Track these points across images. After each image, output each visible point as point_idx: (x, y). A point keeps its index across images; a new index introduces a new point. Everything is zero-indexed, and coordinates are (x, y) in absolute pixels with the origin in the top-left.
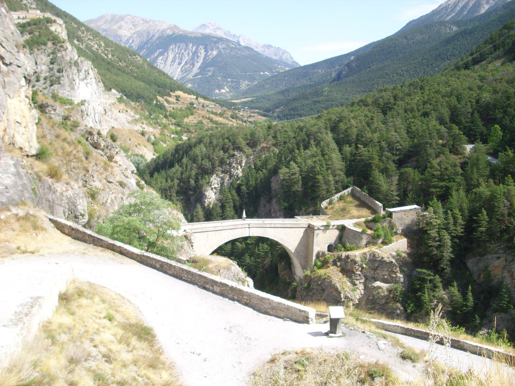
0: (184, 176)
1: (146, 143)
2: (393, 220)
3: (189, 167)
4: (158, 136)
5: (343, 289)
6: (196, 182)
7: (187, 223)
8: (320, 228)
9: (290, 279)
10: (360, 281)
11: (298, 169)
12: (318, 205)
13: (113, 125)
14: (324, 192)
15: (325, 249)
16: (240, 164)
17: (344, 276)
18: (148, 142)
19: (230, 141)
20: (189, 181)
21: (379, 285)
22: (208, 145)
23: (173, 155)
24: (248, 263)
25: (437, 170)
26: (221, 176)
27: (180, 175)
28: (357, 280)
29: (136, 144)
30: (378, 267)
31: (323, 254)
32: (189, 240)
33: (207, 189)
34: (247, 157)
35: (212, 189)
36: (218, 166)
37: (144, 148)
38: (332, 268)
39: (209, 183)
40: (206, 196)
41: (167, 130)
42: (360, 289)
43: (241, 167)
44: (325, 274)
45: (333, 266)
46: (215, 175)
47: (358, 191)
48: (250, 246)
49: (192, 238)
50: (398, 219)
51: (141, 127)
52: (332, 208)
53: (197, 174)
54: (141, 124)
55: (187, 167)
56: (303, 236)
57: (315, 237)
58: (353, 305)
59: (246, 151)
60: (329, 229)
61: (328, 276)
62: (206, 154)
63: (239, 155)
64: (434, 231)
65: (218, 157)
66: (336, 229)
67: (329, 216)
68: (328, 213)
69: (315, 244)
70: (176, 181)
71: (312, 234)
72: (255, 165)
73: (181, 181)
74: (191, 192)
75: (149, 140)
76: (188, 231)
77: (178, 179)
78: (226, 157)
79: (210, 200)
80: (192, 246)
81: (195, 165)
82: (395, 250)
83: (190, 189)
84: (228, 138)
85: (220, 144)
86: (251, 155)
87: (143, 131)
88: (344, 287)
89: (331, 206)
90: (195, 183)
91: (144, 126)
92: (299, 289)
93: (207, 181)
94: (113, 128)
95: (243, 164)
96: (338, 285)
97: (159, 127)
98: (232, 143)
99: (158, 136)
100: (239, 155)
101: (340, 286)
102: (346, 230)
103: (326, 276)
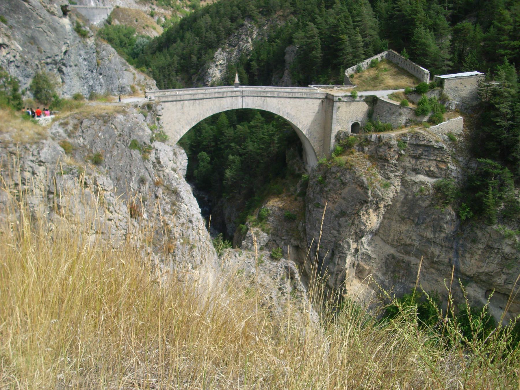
0: (185, 52)
1: (155, 25)
2: (444, 92)
3: (191, 41)
4: (169, 18)
5: (372, 183)
6: (198, 58)
7: (158, 90)
8: (342, 99)
9: (299, 170)
10: (396, 174)
11: (317, 31)
12: (341, 74)
13: (118, 4)
14: (350, 57)
15: (348, 128)
16: (251, 35)
17: (374, 166)
18: (158, 24)
19: (239, 9)
20: (191, 58)
21: (422, 180)
22: (214, 15)
23: (177, 32)
24: (251, 151)
26: (228, 50)
27: (180, 51)
28: (392, 172)
29: (143, 25)
30: (421, 154)
31: (346, 134)
32: (154, 112)
33: (211, 65)
34: (260, 27)
35: (217, 66)
36: (225, 38)
37: (152, 30)
38: (356, 154)
39: (212, 59)
40: (209, 74)
41: (181, 12)
42: (396, 184)
43: (252, 40)
44: (347, 163)
45: (359, 151)
46: (220, 49)
47: (395, 55)
48: (254, 130)
49: (159, 108)
50: (451, 89)
51: (151, 7)
52: (360, 77)
53: (200, 49)
54: (150, 5)
55: (189, 41)
56: (319, 110)
57: (334, 111)
58: (385, 206)
59: (258, 20)
60: (353, 101)
61: (351, 166)
62: (211, 25)
63: (249, 25)
64: (504, 105)
65: (224, 27)
66: (364, 101)
67: (355, 87)
68: (354, 83)
69: (334, 121)
70: (176, 58)
71: (330, 108)
72: (269, 36)
73: (181, 58)
74: (192, 71)
75: (158, 22)
76: (153, 98)
77: (178, 56)
78: (234, 27)
79: (214, 79)
80: (158, 119)
81: (198, 38)
82: (446, 132)
83: (192, 67)
84: (238, 6)
85: (227, 13)
86: (264, 25)
87: (152, 12)
88: (373, 181)
89: (359, 74)
90: (198, 59)
91: (154, 7)
92: (311, 183)
93: (211, 57)
94: (118, 7)
95: (254, 36)
96: (364, 179)
97: (172, 9)
98: (242, 11)
99: (169, 18)
100: (249, 25)
101: (367, 179)
103: (348, 165)
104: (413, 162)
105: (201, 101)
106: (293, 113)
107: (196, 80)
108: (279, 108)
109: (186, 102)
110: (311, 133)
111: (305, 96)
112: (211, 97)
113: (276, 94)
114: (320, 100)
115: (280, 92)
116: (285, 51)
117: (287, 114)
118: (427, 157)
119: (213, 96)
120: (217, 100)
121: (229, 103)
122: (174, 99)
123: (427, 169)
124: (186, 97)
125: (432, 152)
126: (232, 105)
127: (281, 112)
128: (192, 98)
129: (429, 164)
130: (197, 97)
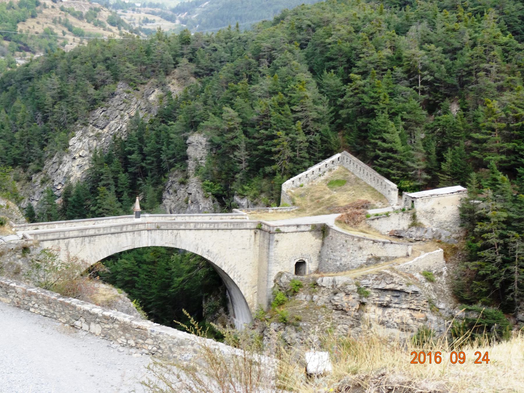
8: (282, 229)
25: (500, 120)
30: (390, 302)
46: (79, 133)
66: (310, 231)
102: (331, 234)
104: (379, 311)
105: (92, 239)
106: (215, 251)
107: (39, 181)
108: (197, 245)
109: (72, 241)
110: (240, 276)
111: (232, 227)
112: (105, 232)
113: (192, 226)
114: (252, 232)
115: (198, 223)
116: (188, 142)
117: (208, 251)
118: (397, 306)
119: (109, 232)
120: (113, 236)
121: (130, 240)
122: (56, 237)
123: (399, 321)
124: (72, 234)
125: (404, 299)
126: (133, 243)
127: (200, 249)
128: (81, 234)
129: (401, 313)
130: (87, 233)
